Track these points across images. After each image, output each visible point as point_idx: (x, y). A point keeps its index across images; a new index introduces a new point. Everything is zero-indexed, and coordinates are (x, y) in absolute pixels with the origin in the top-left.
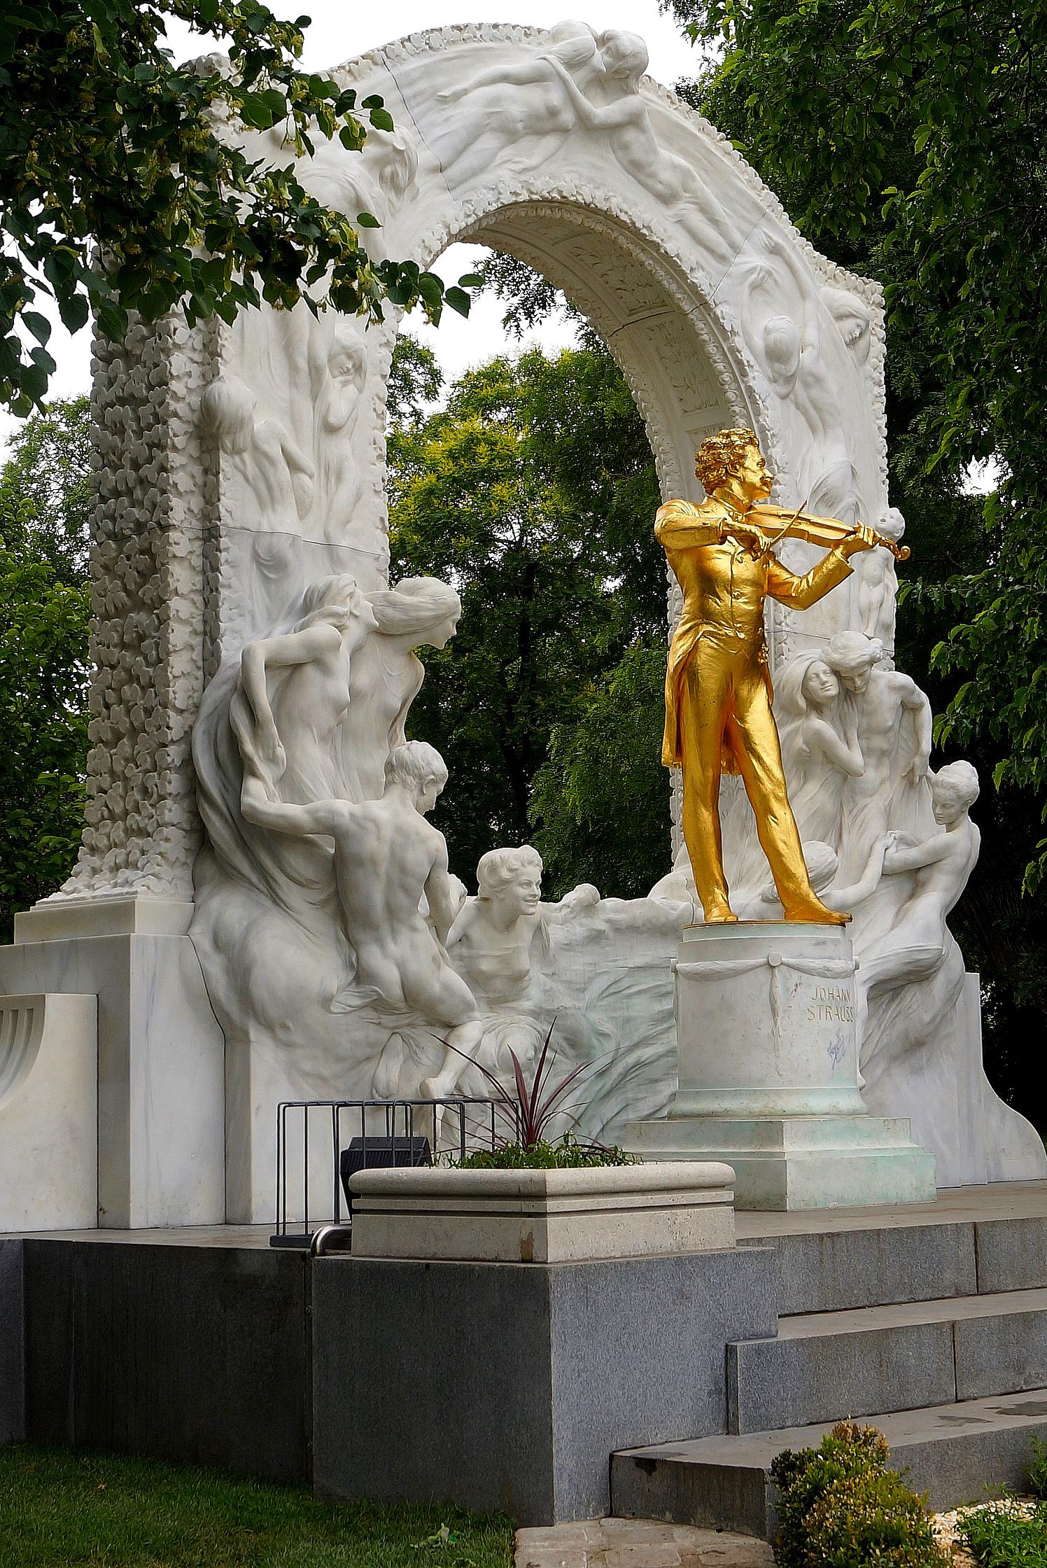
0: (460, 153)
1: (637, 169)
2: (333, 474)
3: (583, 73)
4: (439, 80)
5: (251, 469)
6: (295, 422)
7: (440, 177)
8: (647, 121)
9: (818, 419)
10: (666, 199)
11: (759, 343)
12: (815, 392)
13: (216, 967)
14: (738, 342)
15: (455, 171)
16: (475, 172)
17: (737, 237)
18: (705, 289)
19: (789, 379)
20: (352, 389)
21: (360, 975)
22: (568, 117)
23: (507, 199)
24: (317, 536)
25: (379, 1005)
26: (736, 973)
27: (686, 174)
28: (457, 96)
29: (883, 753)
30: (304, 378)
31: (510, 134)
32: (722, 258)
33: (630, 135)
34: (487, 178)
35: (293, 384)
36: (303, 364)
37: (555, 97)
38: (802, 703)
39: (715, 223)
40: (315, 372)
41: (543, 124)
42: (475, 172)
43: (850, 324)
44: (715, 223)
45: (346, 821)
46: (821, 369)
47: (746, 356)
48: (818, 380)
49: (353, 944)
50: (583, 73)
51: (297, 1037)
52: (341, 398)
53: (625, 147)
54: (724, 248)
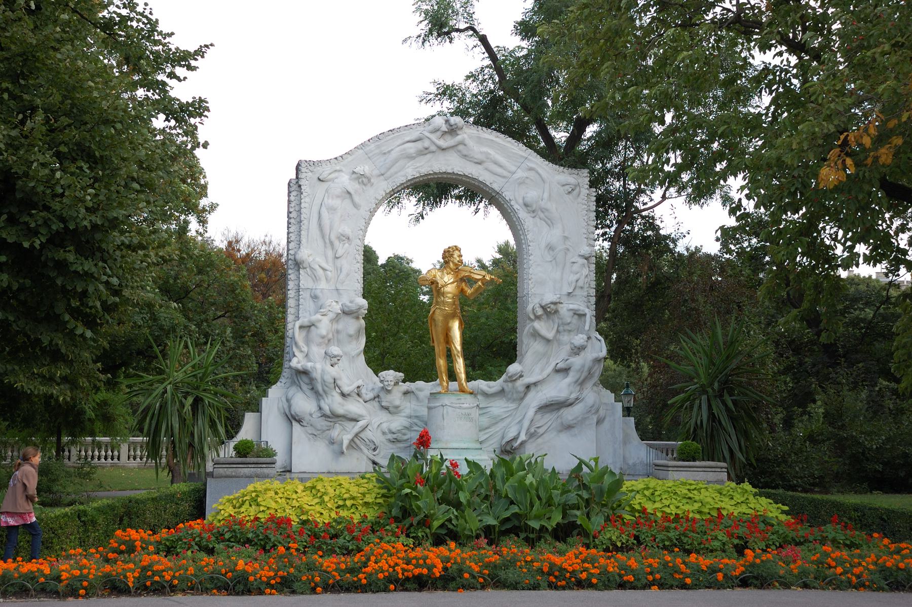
0: (390, 169)
1: (465, 156)
2: (339, 270)
3: (439, 133)
4: (383, 148)
5: (309, 272)
6: (326, 257)
7: (382, 177)
8: (468, 141)
9: (550, 222)
10: (480, 164)
11: (521, 201)
12: (546, 214)
13: (286, 406)
14: (512, 203)
15: (388, 174)
16: (396, 173)
17: (513, 168)
18: (497, 189)
19: (533, 212)
20: (347, 245)
21: (320, 409)
22: (433, 148)
24: (333, 288)
25: (324, 416)
26: (435, 407)
27: (487, 154)
28: (389, 152)
29: (570, 331)
30: (328, 245)
31: (411, 157)
32: (504, 177)
33: (461, 147)
34: (402, 173)
35: (325, 247)
36: (327, 241)
37: (427, 143)
38: (532, 317)
39: (501, 166)
40: (332, 243)
41: (425, 151)
42: (396, 173)
43: (567, 187)
44: (501, 166)
45: (309, 369)
46: (549, 205)
47: (516, 207)
48: (547, 210)
49: (318, 400)
50: (439, 133)
51: (305, 424)
52: (341, 249)
53: (459, 151)
54: (505, 173)
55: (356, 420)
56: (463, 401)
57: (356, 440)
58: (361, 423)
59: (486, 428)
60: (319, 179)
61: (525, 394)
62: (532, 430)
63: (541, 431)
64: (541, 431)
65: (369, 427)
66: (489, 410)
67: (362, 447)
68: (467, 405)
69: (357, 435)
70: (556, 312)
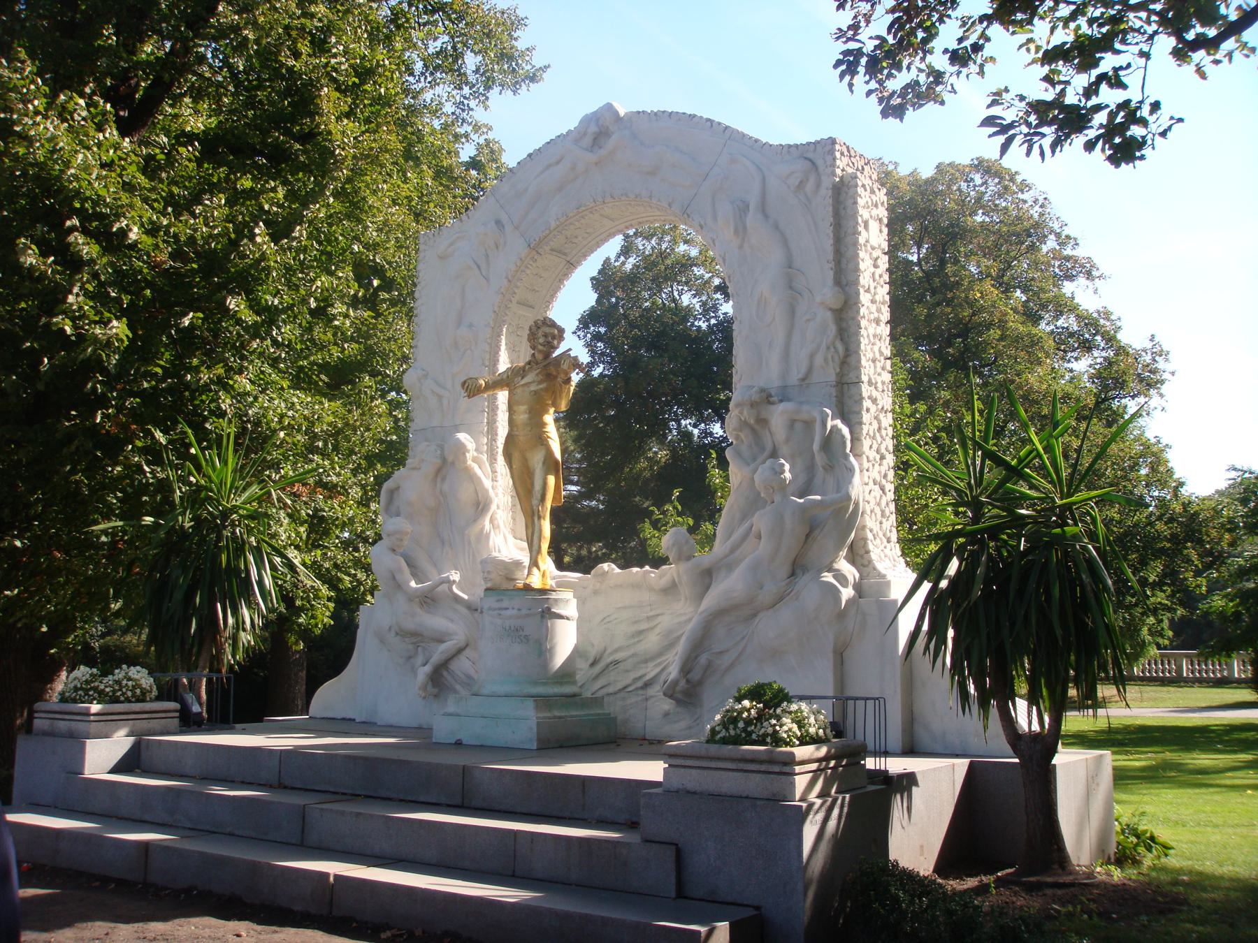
23: (553, 225)
55: (441, 641)
56: (505, 604)
57: (445, 673)
58: (443, 647)
59: (660, 654)
60: (440, 257)
61: (707, 588)
62: (703, 660)
63: (727, 660)
64: (727, 660)
65: (467, 652)
66: (660, 619)
67: (458, 687)
68: (515, 612)
69: (443, 666)
70: (763, 422)
